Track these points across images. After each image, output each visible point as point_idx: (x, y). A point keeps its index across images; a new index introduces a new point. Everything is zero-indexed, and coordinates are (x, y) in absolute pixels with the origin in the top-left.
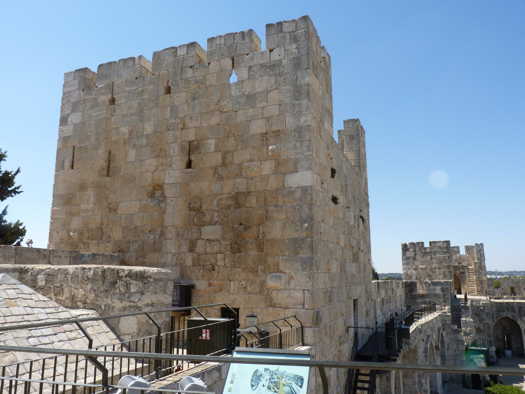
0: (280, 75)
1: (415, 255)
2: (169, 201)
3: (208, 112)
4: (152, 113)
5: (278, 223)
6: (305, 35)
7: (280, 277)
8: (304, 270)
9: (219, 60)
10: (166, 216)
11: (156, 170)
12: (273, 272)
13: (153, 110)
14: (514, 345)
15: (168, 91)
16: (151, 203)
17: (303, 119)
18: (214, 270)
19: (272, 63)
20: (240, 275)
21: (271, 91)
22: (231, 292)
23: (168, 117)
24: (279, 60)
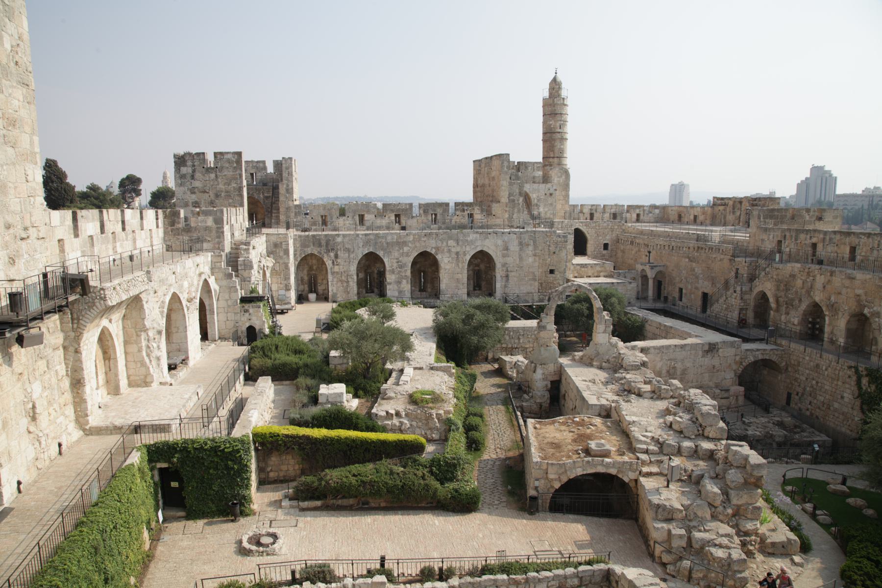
1: (194, 171)
14: (320, 288)
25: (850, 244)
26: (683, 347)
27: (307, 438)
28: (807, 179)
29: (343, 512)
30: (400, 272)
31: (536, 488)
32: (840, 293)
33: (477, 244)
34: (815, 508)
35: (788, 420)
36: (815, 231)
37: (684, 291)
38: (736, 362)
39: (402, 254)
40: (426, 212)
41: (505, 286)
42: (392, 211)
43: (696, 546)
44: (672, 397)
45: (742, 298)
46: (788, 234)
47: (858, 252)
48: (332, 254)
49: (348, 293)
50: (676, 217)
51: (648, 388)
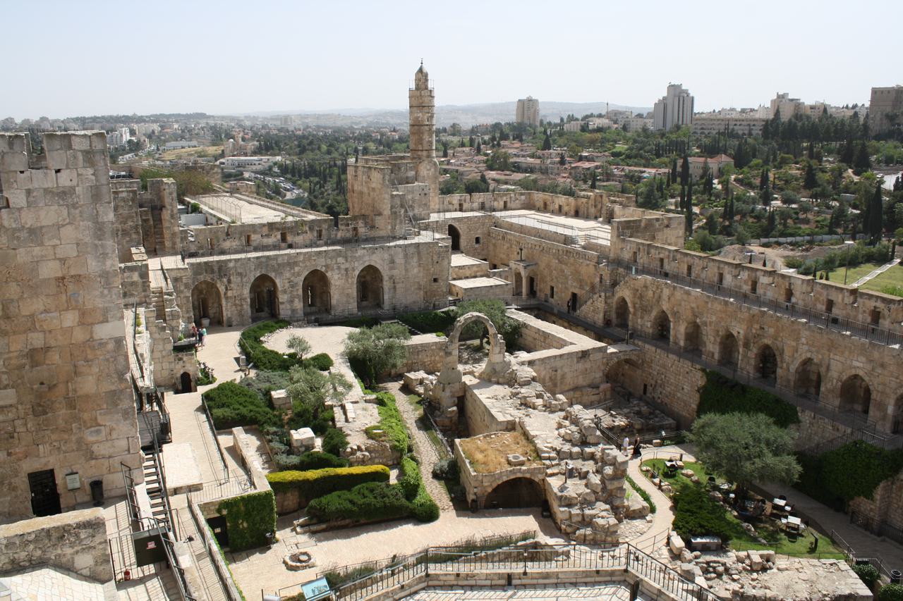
0: (74, 206)
5: (90, 378)
7: (98, 432)
8: (125, 419)
12: (91, 427)
14: (211, 312)
17: (109, 263)
18: (13, 437)
19: (61, 189)
21: (63, 226)
22: (41, 455)
24: (71, 187)
25: (687, 262)
26: (561, 356)
28: (664, 98)
29: (343, 530)
30: (292, 291)
31: (475, 494)
32: (680, 305)
33: (365, 259)
34: (660, 481)
35: (644, 409)
36: (662, 248)
37: (555, 289)
38: (603, 364)
39: (293, 274)
40: (311, 229)
41: (393, 297)
42: (278, 229)
43: (587, 520)
44: (561, 410)
46: (641, 247)
47: (693, 270)
48: (225, 280)
49: (243, 316)
51: (539, 402)
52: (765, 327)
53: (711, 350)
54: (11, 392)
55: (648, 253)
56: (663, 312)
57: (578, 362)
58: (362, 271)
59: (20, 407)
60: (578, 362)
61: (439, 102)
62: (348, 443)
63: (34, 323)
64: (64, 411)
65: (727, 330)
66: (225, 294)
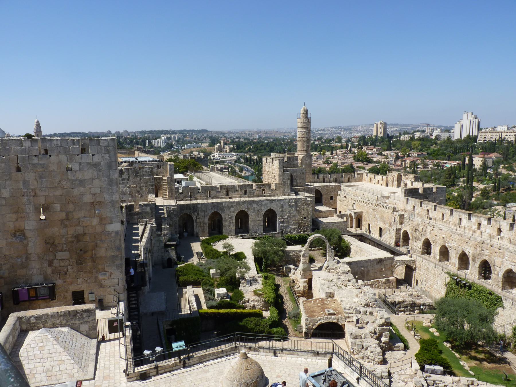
0: (100, 171)
1: (129, 177)
2: (30, 239)
3: (53, 187)
4: (7, 184)
6: (114, 150)
7: (106, 274)
8: (118, 269)
9: (58, 155)
10: (28, 248)
11: (17, 220)
13: (8, 182)
15: (19, 170)
16: (16, 241)
17: (114, 196)
18: (66, 274)
19: (94, 163)
20: (83, 275)
21: (94, 179)
23: (22, 187)
26: (366, 261)
27: (219, 313)
37: (371, 225)
42: (224, 189)
45: (397, 233)
46: (417, 203)
47: (445, 216)
50: (369, 180)
52: (484, 250)
53: (454, 262)
54: (67, 253)
55: (421, 206)
56: (428, 239)
57: (377, 264)
58: (267, 211)
59: (71, 260)
60: (377, 264)
61: (313, 126)
62: (244, 297)
63: (79, 222)
64: (90, 264)
65: (463, 251)
66: (196, 220)
